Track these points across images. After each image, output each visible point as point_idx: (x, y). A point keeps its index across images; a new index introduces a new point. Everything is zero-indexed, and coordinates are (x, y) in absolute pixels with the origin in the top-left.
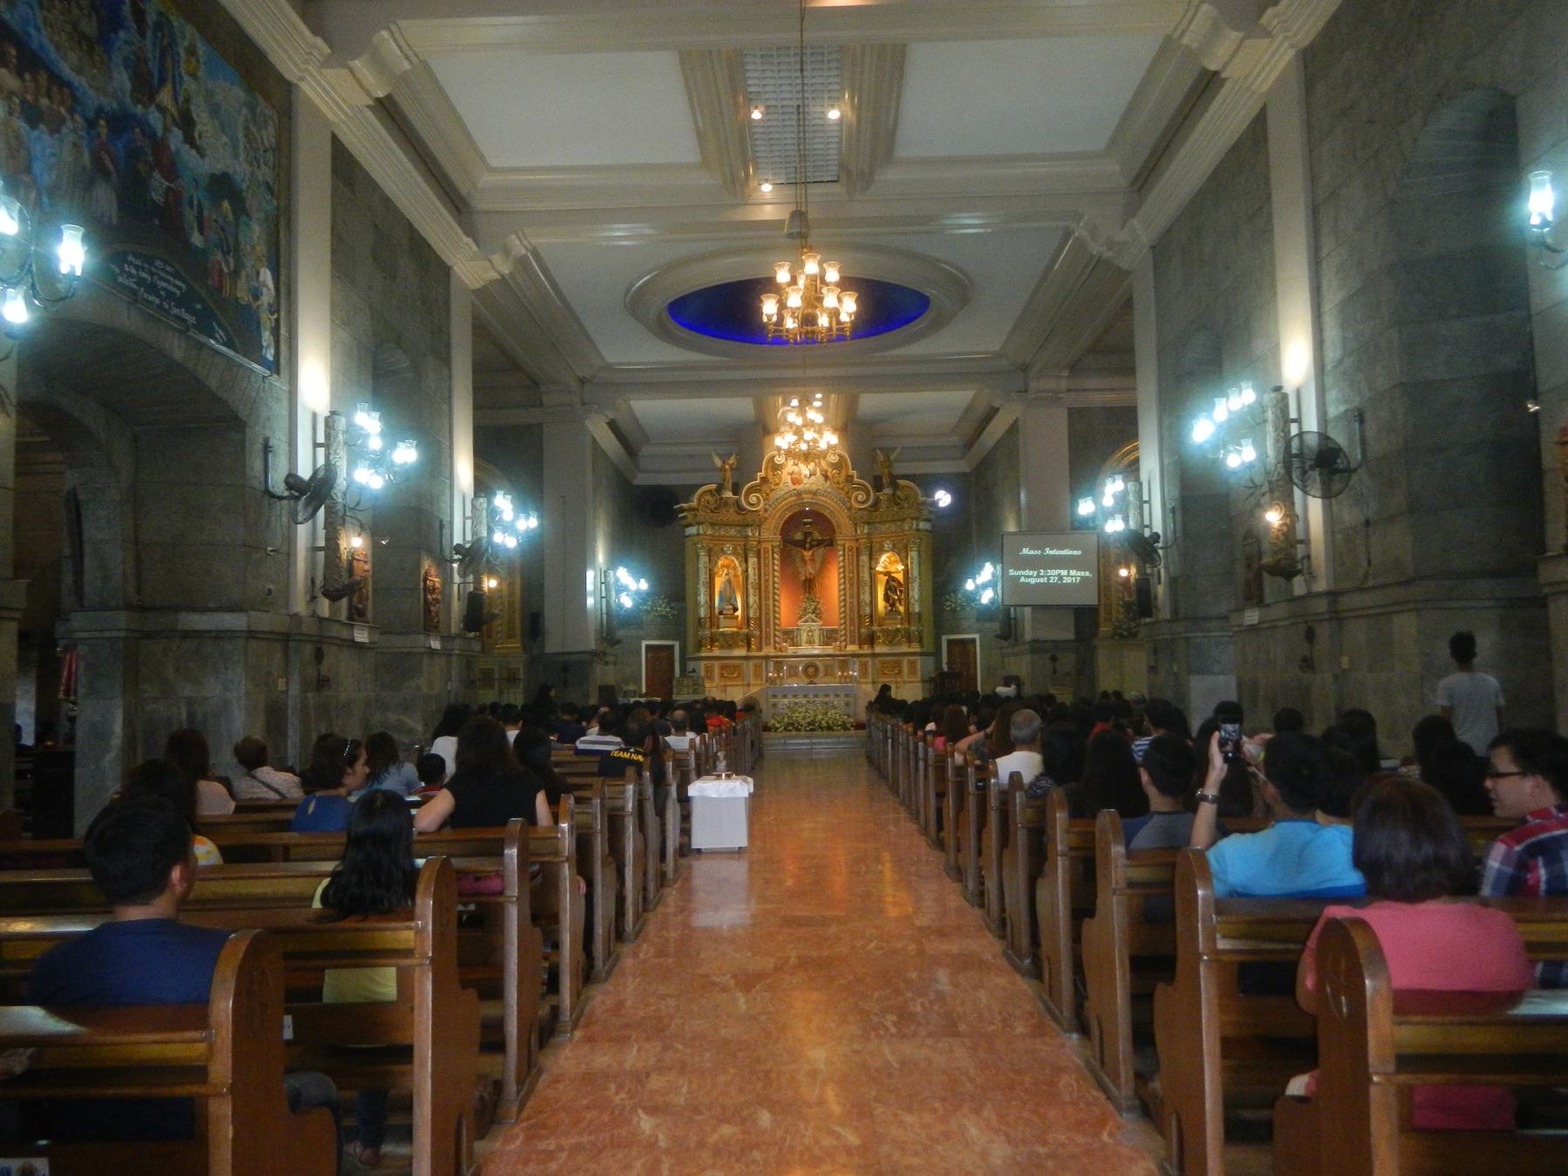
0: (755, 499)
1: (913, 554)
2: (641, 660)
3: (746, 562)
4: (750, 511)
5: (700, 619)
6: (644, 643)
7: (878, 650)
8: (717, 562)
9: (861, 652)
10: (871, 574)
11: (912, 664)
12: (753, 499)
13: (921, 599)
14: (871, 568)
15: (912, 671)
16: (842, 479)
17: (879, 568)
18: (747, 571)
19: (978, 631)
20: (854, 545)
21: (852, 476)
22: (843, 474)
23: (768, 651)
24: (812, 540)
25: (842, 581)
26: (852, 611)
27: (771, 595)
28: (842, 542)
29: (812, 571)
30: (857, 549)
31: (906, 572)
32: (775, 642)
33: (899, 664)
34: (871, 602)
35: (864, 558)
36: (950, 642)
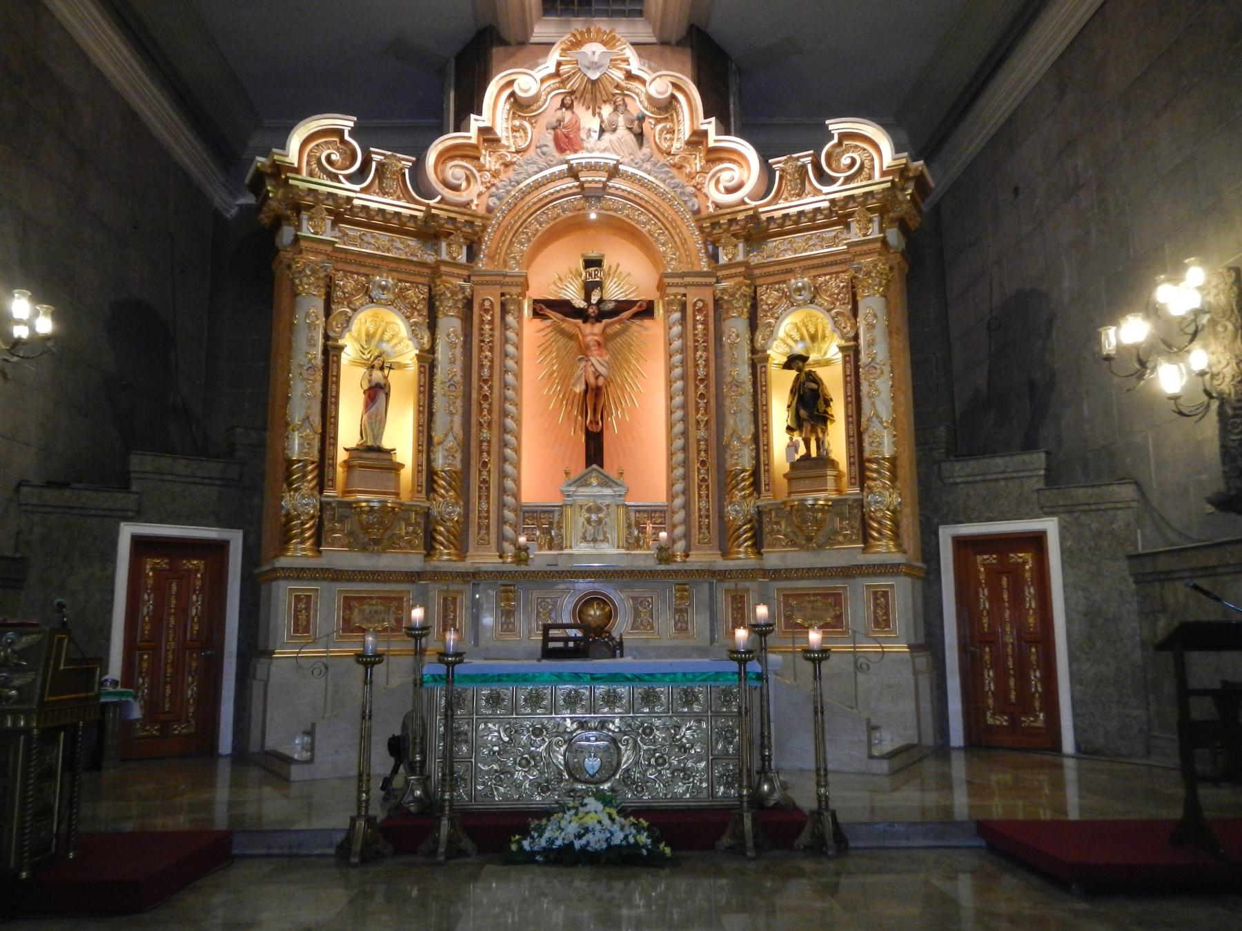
0: (461, 173)
1: (872, 304)
2: (112, 579)
3: (432, 327)
4: (443, 200)
5: (290, 463)
6: (127, 531)
7: (773, 558)
8: (348, 320)
9: (730, 564)
10: (753, 366)
11: (881, 599)
12: (454, 170)
13: (894, 422)
14: (754, 351)
15: (882, 620)
16: (677, 145)
17: (777, 353)
18: (432, 350)
19: (1047, 511)
20: (707, 295)
21: (705, 133)
22: (685, 131)
23: (484, 558)
24: (601, 301)
25: (679, 384)
26: (703, 463)
27: (495, 416)
28: (682, 290)
29: (602, 370)
30: (717, 302)
31: (852, 353)
32: (502, 537)
33: (836, 599)
34: (756, 438)
35: (736, 327)
36: (961, 543)
